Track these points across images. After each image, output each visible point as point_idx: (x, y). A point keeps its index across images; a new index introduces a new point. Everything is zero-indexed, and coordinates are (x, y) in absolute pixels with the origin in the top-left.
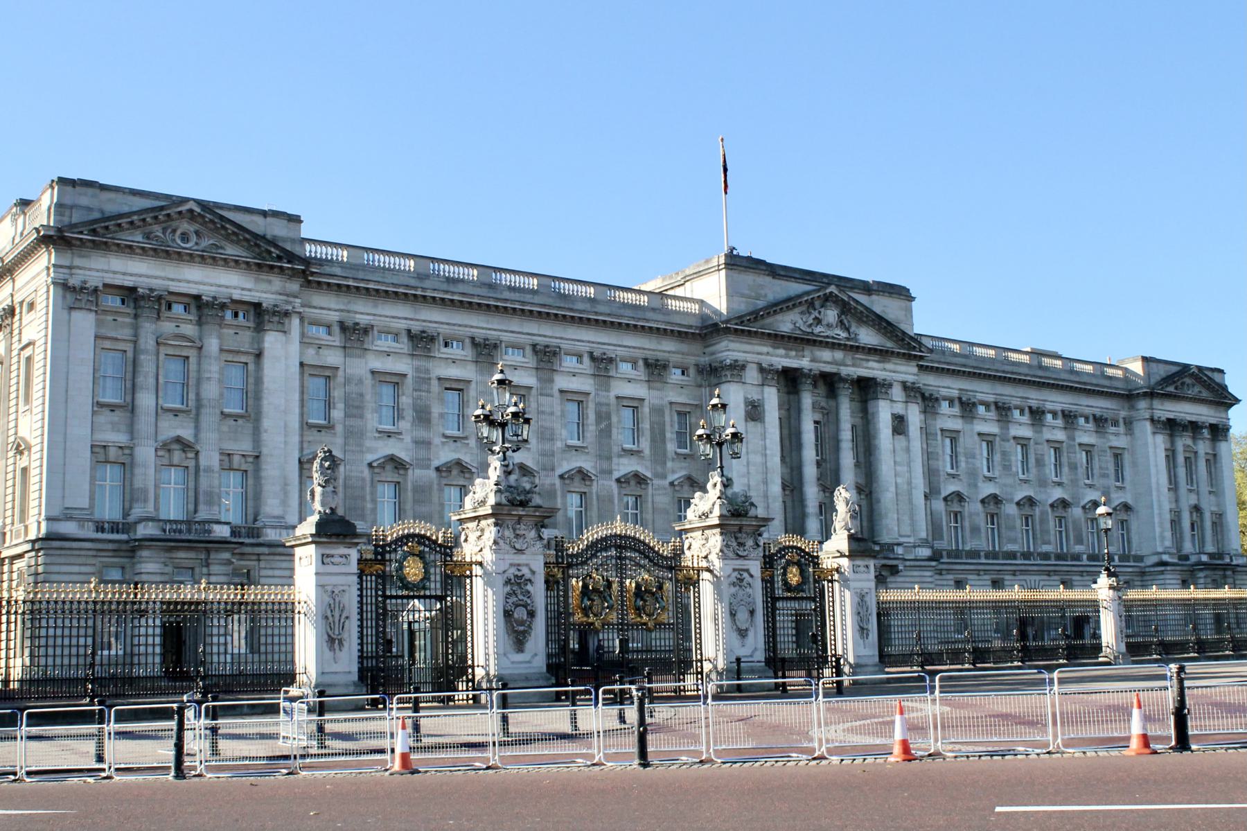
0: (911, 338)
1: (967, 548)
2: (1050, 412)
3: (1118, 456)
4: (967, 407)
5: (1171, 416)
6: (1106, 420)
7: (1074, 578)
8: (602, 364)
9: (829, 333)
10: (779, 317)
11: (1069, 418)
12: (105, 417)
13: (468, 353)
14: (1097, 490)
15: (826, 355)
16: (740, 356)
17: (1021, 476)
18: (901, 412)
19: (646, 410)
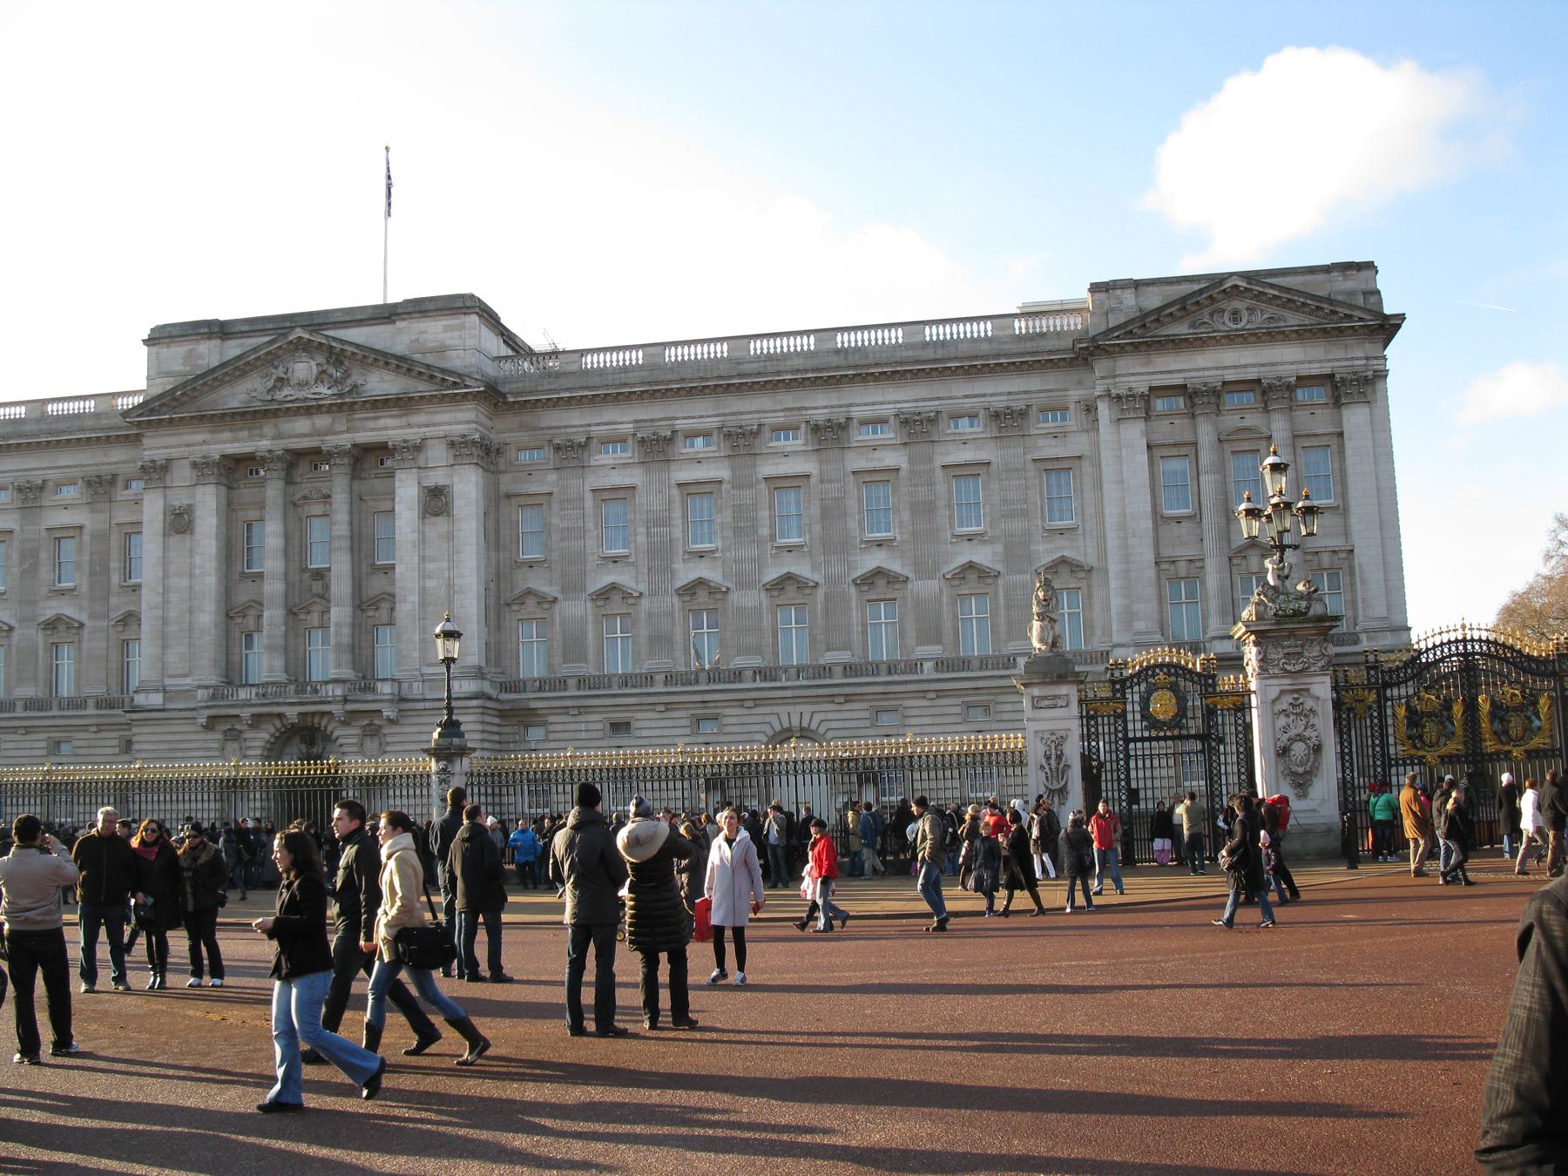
0: (443, 371)
1: (646, 667)
2: (864, 423)
4: (656, 448)
5: (1176, 380)
6: (1023, 414)
7: (908, 703)
10: (226, 391)
11: (917, 427)
14: (991, 541)
15: (302, 425)
16: (159, 455)
18: (441, 482)
19: (86, 538)
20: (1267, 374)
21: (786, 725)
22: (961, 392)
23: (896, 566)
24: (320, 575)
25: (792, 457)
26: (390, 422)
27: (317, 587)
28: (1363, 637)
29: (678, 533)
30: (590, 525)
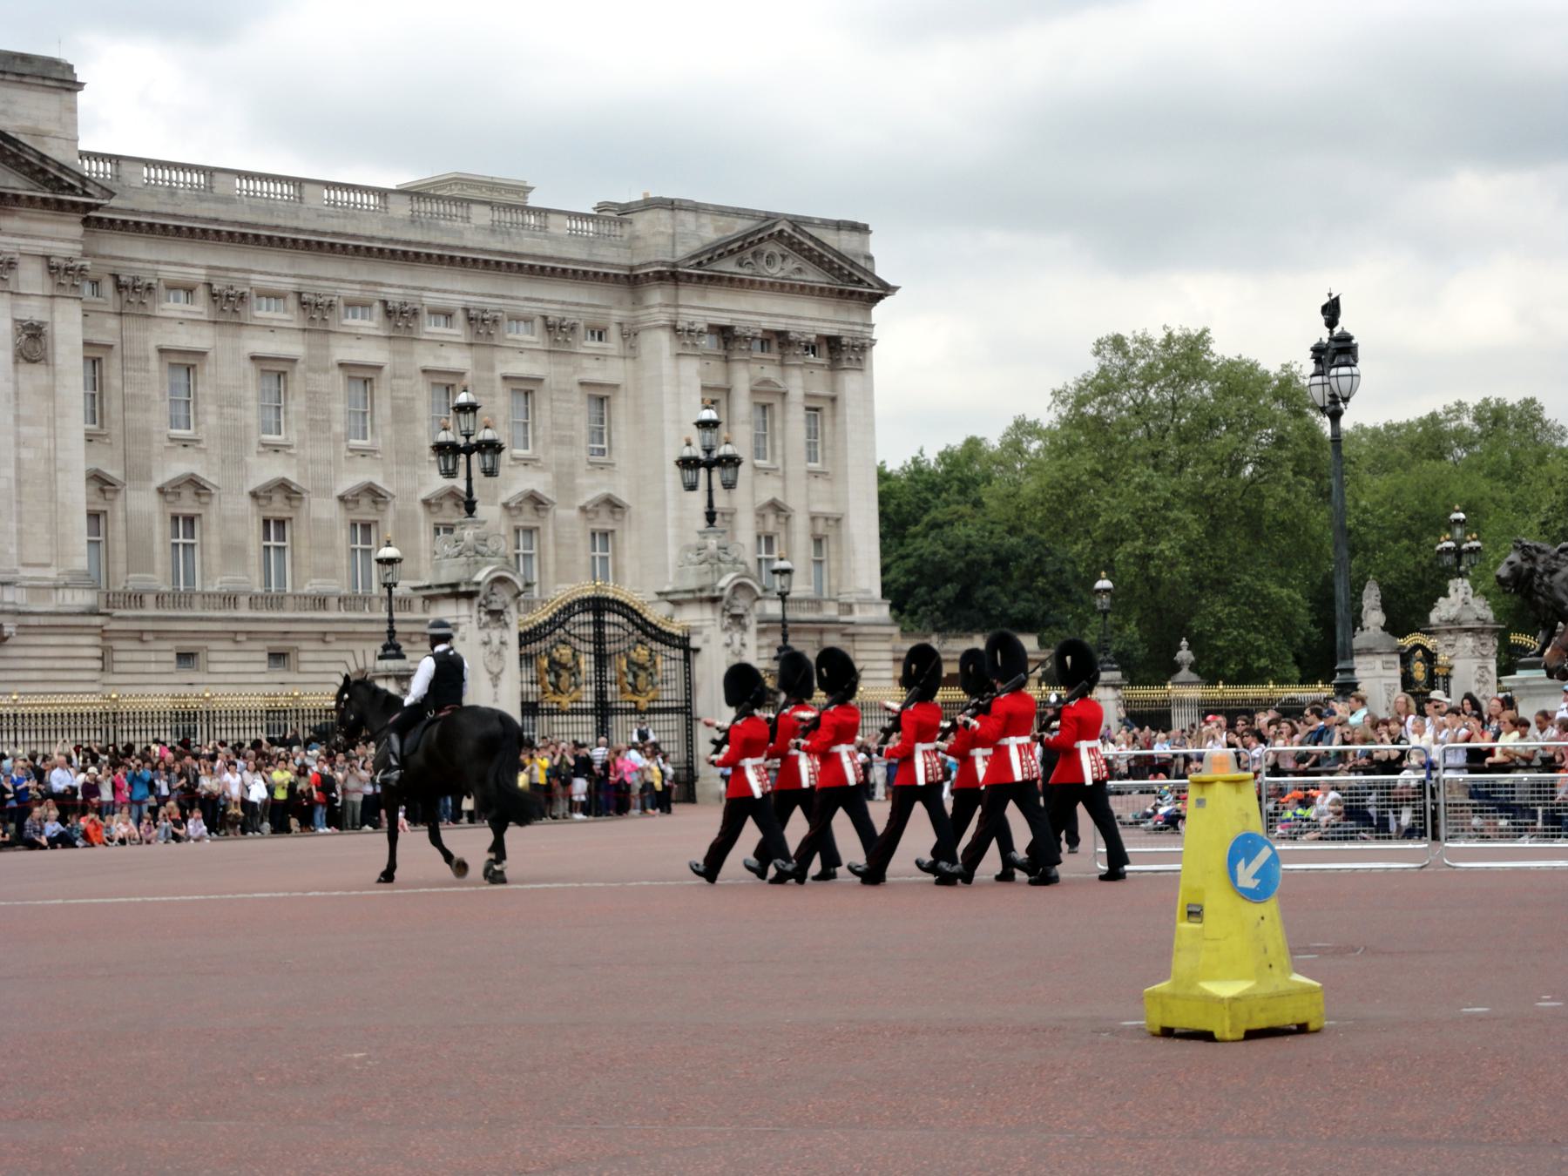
0: (61, 167)
2: (434, 312)
3: (600, 398)
4: (228, 305)
5: (724, 320)
6: (573, 328)
11: (481, 325)
17: (354, 442)
21: (361, 666)
25: (361, 340)
28: (856, 608)
29: (251, 416)
30: (157, 396)
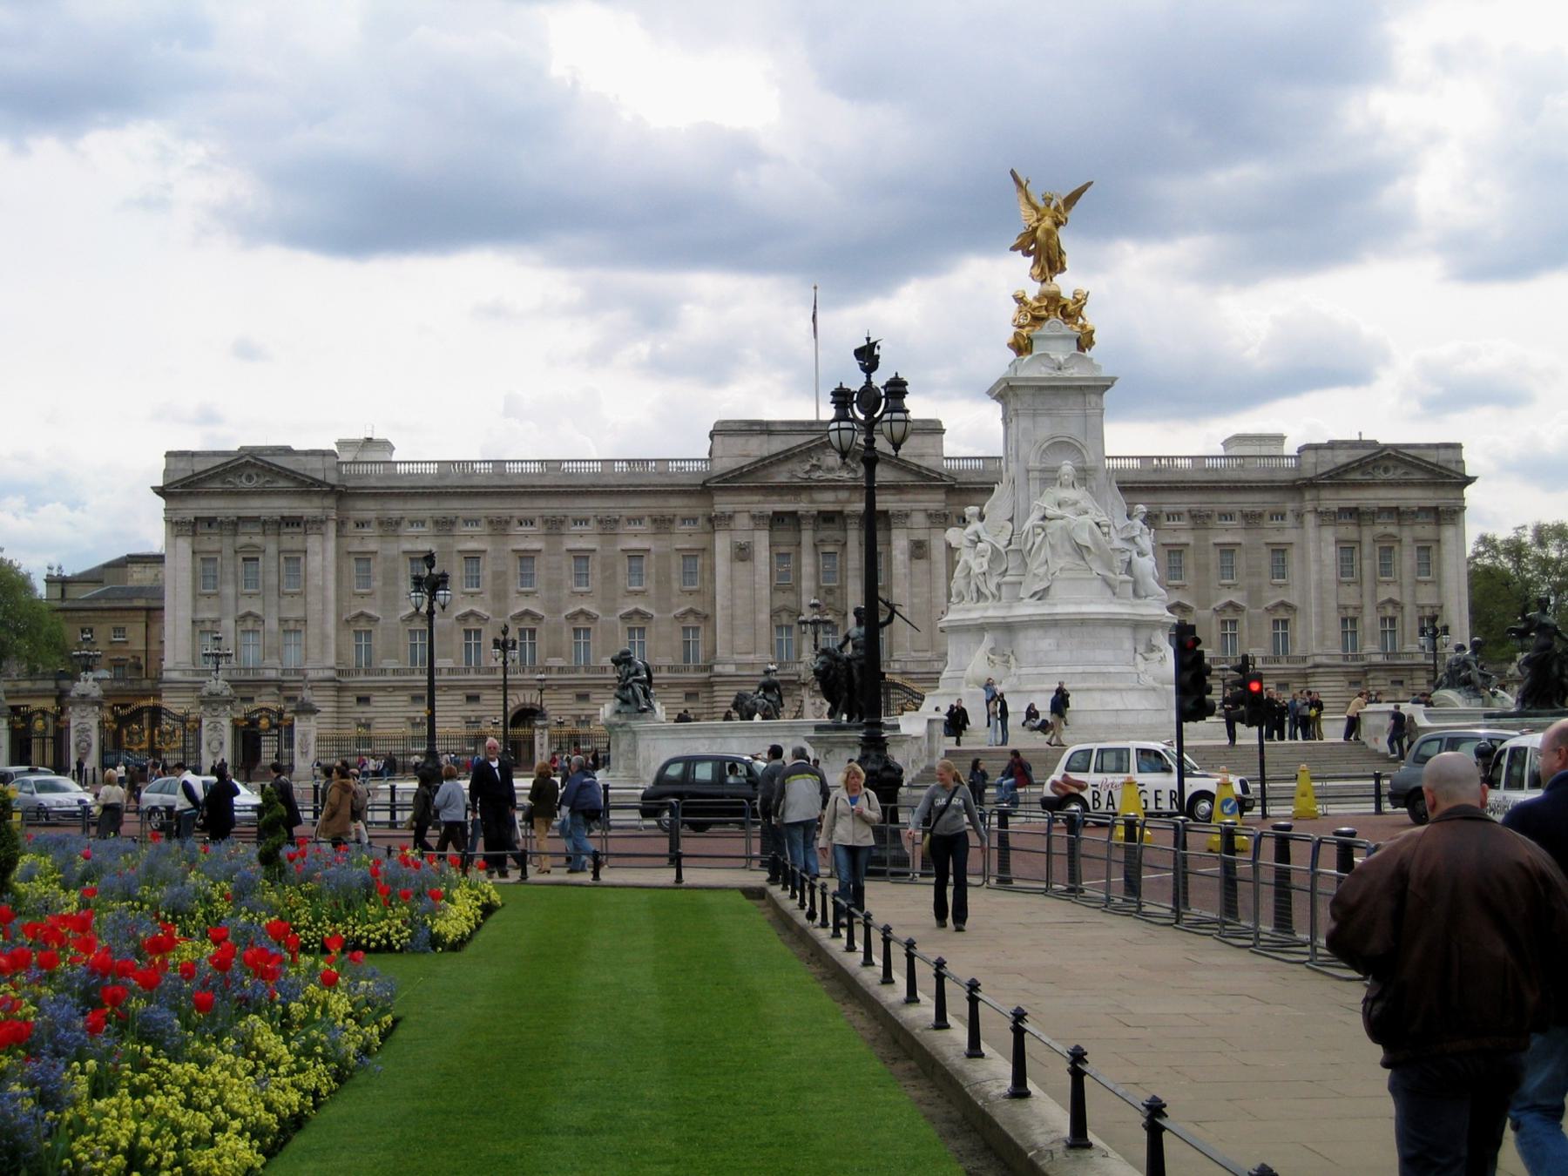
5: (1353, 504)
6: (1261, 515)
8: (608, 525)
9: (830, 476)
10: (774, 470)
12: (203, 602)
13: (482, 529)
14: (1241, 589)
15: (829, 496)
16: (728, 509)
20: (1403, 505)
22: (1226, 501)
23: (1187, 602)
24: (830, 591)
26: (890, 498)
27: (830, 599)
